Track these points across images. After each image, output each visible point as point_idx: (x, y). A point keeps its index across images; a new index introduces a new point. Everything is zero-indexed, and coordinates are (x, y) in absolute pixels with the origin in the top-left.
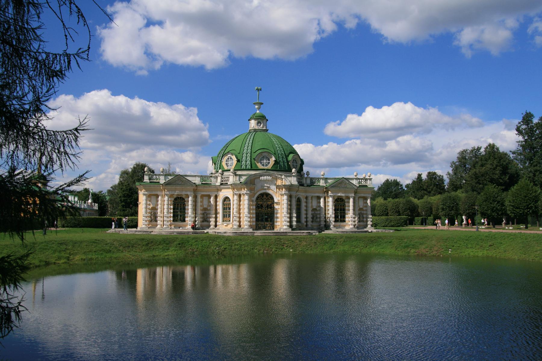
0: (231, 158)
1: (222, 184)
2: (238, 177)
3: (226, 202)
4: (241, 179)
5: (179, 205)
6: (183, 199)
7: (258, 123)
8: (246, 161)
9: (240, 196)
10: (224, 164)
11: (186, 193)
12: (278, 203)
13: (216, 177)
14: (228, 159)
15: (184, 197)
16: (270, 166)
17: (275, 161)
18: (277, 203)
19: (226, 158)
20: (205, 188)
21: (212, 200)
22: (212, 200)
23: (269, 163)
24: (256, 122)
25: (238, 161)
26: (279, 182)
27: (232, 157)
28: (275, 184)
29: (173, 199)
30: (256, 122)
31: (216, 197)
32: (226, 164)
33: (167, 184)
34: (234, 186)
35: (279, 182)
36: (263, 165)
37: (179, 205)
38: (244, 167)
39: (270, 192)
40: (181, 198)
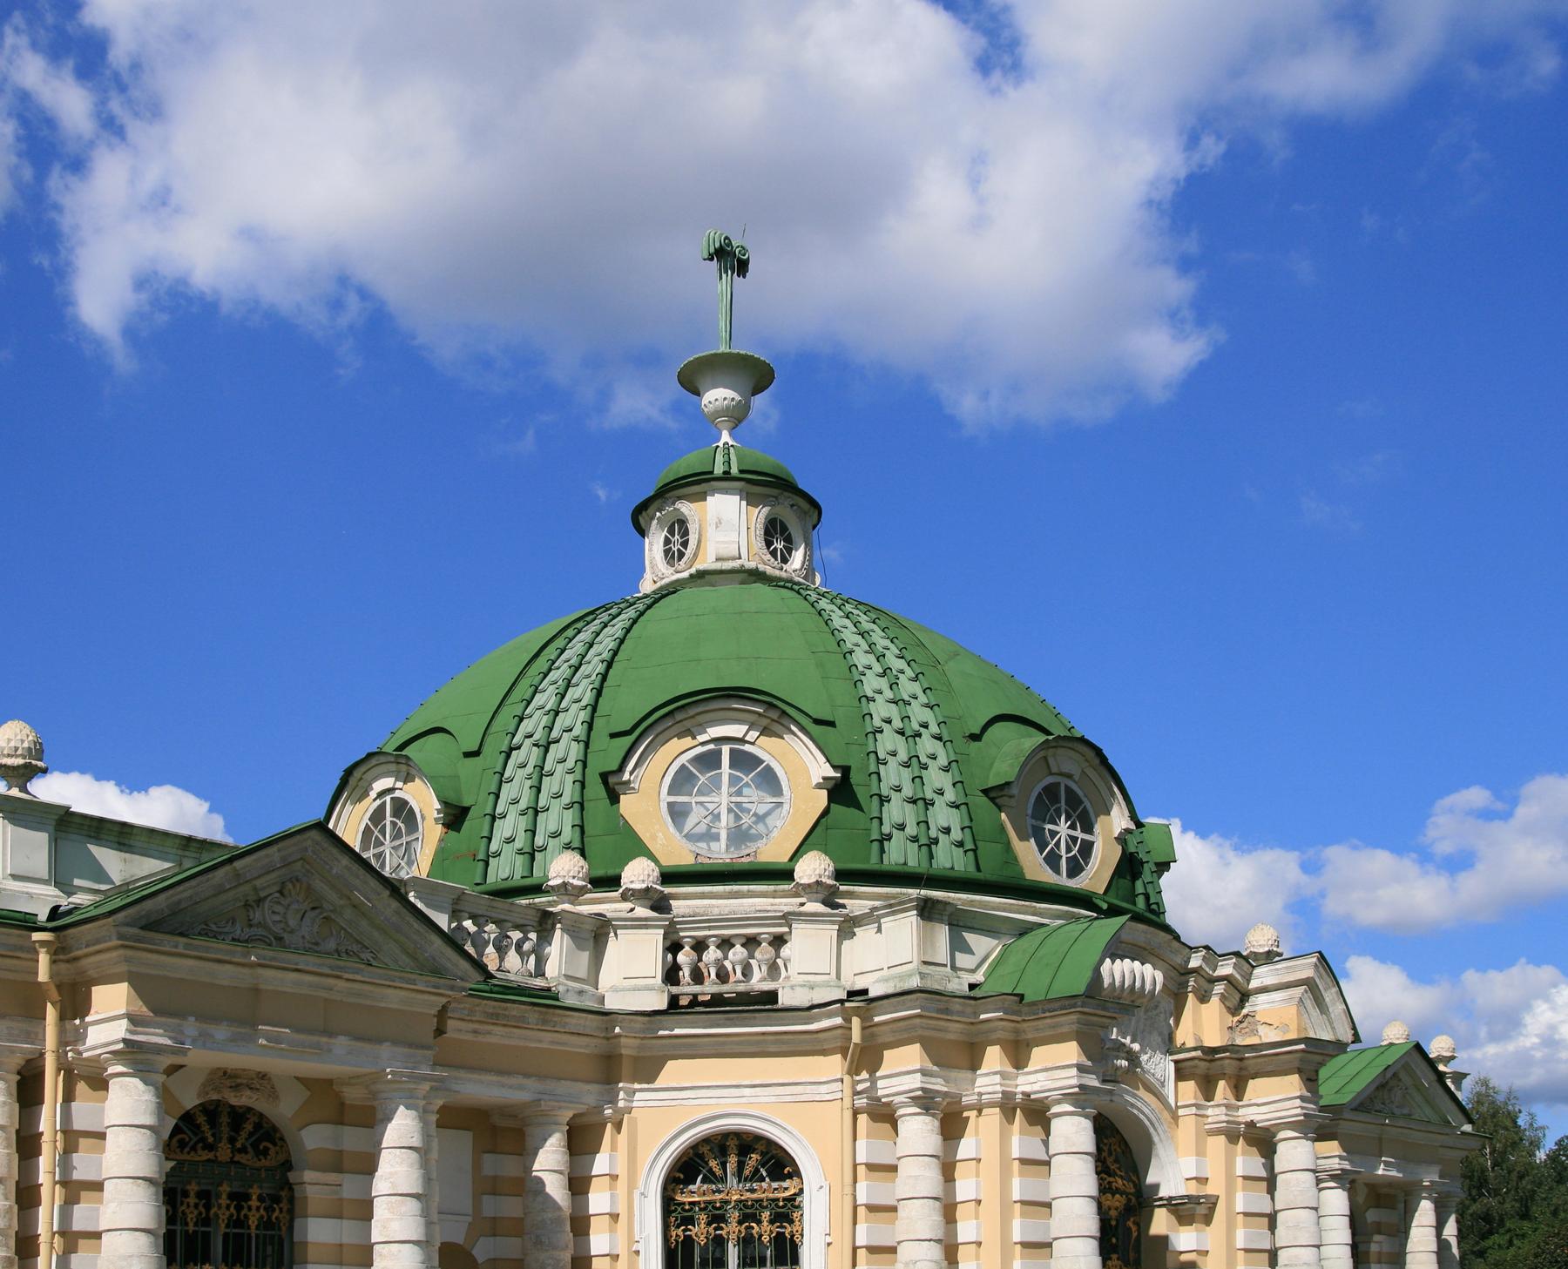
0: (744, 761)
1: (674, 1001)
2: (942, 933)
3: (696, 1193)
4: (963, 960)
5: (223, 1211)
6: (266, 1135)
7: (774, 530)
8: (925, 804)
9: (952, 1125)
10: (645, 806)
11: (338, 1060)
12: (1194, 1210)
13: (596, 935)
14: (709, 761)
15: (283, 1110)
16: (1096, 875)
17: (1121, 840)
18: (1194, 1210)
19: (676, 752)
20: (498, 1036)
21: (549, 1160)
22: (549, 1160)
23: (1087, 848)
24: (759, 515)
25: (841, 791)
26: (1202, 1024)
27: (764, 748)
28: (1169, 1045)
29: (171, 1123)
30: (759, 515)
31: (582, 1141)
32: (678, 814)
33: (153, 925)
34: (860, 1027)
35: (1202, 1024)
36: (1052, 861)
37: (223, 1211)
38: (900, 853)
39: (1142, 1104)
40: (239, 1116)
